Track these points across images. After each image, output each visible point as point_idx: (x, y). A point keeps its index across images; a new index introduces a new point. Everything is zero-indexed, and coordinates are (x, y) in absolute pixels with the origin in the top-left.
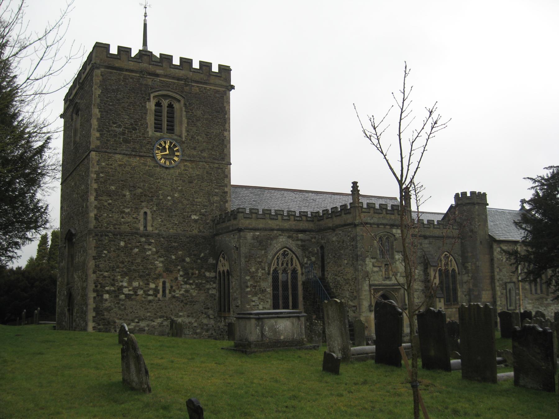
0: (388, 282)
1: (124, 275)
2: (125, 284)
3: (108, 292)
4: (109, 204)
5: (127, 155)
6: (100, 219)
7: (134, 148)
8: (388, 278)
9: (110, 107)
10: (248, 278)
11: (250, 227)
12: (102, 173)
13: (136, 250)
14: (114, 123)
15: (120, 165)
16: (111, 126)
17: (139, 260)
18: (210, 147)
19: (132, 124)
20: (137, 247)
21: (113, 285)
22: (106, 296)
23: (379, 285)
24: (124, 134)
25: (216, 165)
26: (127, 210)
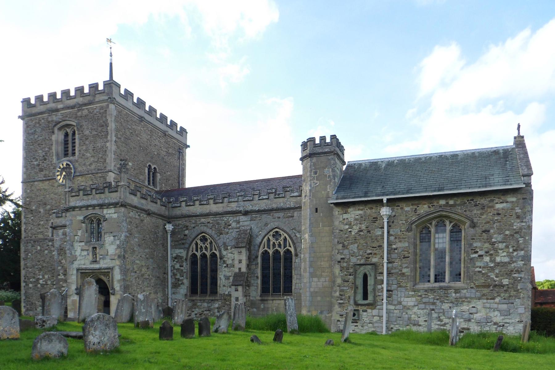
0: (96, 266)
1: (40, 270)
2: (41, 277)
3: (31, 283)
4: (32, 220)
5: (41, 181)
6: (27, 231)
7: (45, 175)
8: (96, 261)
9: (31, 147)
10: (59, 268)
11: (61, 225)
12: (28, 197)
13: (46, 252)
14: (34, 158)
15: (38, 190)
16: (32, 161)
17: (47, 260)
18: (96, 160)
19: (44, 156)
20: (47, 249)
21: (34, 278)
22: (31, 285)
23: (86, 269)
24: (38, 165)
25: (100, 175)
26: (42, 223)
